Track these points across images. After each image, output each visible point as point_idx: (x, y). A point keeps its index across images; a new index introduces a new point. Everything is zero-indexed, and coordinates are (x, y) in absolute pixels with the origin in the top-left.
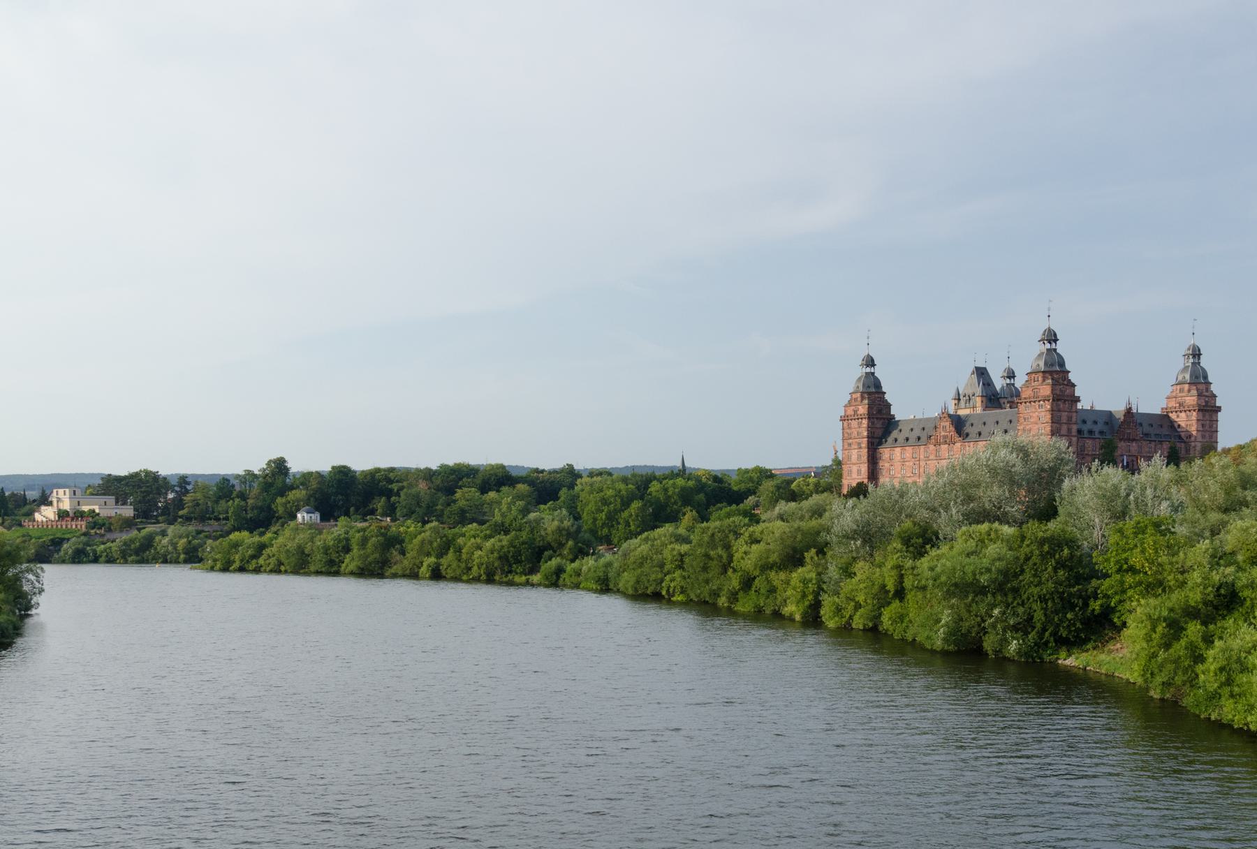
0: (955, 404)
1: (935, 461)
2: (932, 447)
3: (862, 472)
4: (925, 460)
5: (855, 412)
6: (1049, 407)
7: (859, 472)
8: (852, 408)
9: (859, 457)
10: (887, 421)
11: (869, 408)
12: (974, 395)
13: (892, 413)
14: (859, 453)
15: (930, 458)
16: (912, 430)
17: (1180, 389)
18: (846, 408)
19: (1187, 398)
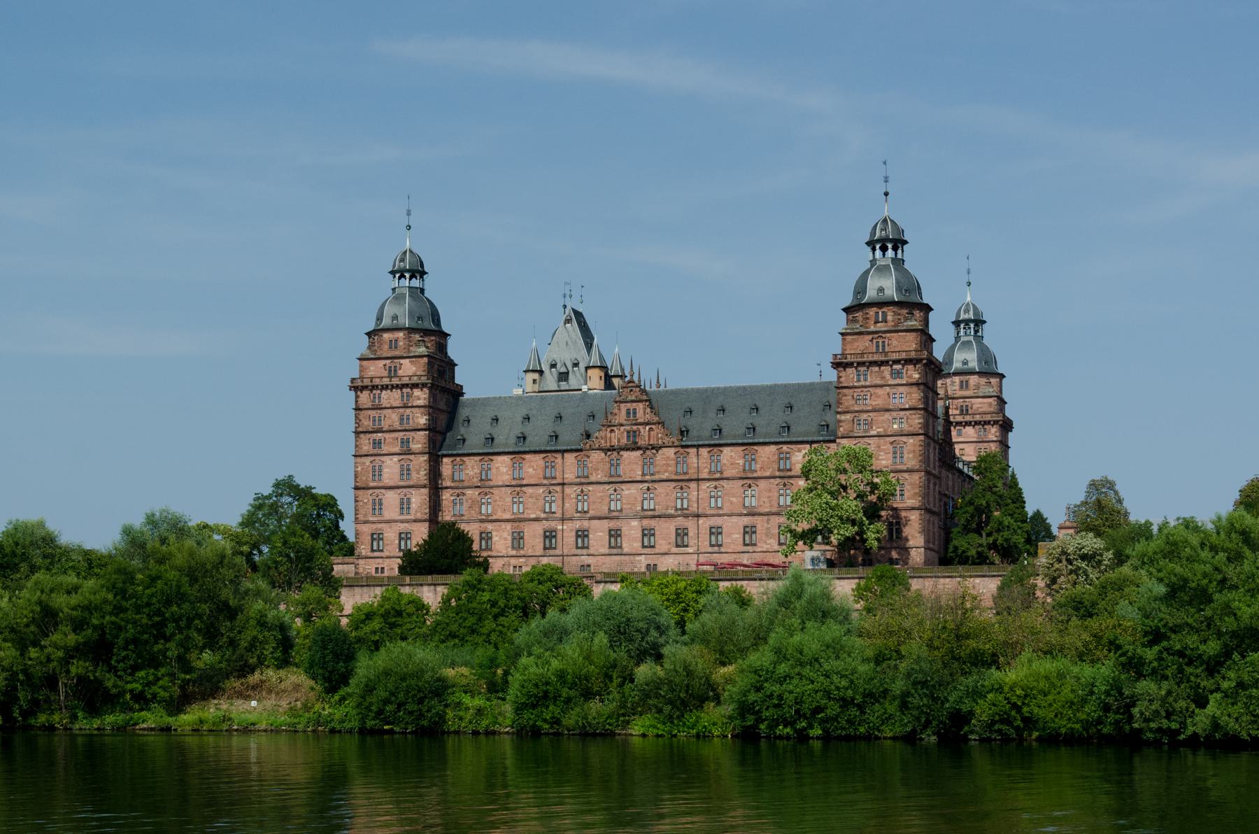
0: (534, 381)
1: (607, 487)
2: (597, 456)
3: (413, 506)
4: (582, 484)
5: (392, 372)
6: (917, 376)
7: (405, 505)
8: (384, 362)
9: (405, 471)
10: (451, 398)
11: (429, 363)
12: (576, 365)
13: (457, 381)
14: (402, 462)
15: (593, 479)
16: (528, 418)
17: (962, 382)
18: (365, 363)
19: (973, 400)
